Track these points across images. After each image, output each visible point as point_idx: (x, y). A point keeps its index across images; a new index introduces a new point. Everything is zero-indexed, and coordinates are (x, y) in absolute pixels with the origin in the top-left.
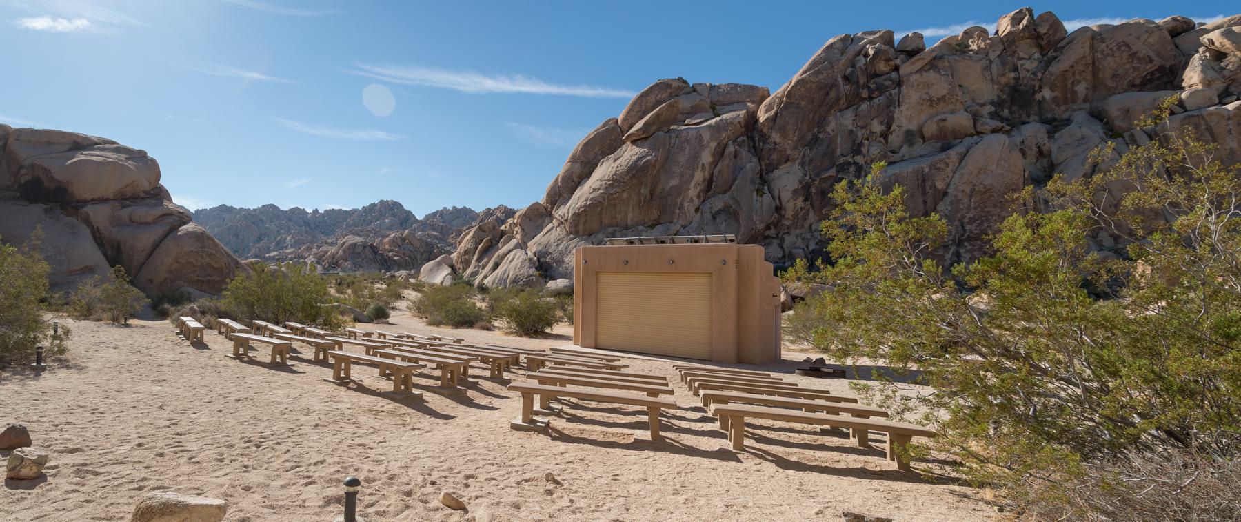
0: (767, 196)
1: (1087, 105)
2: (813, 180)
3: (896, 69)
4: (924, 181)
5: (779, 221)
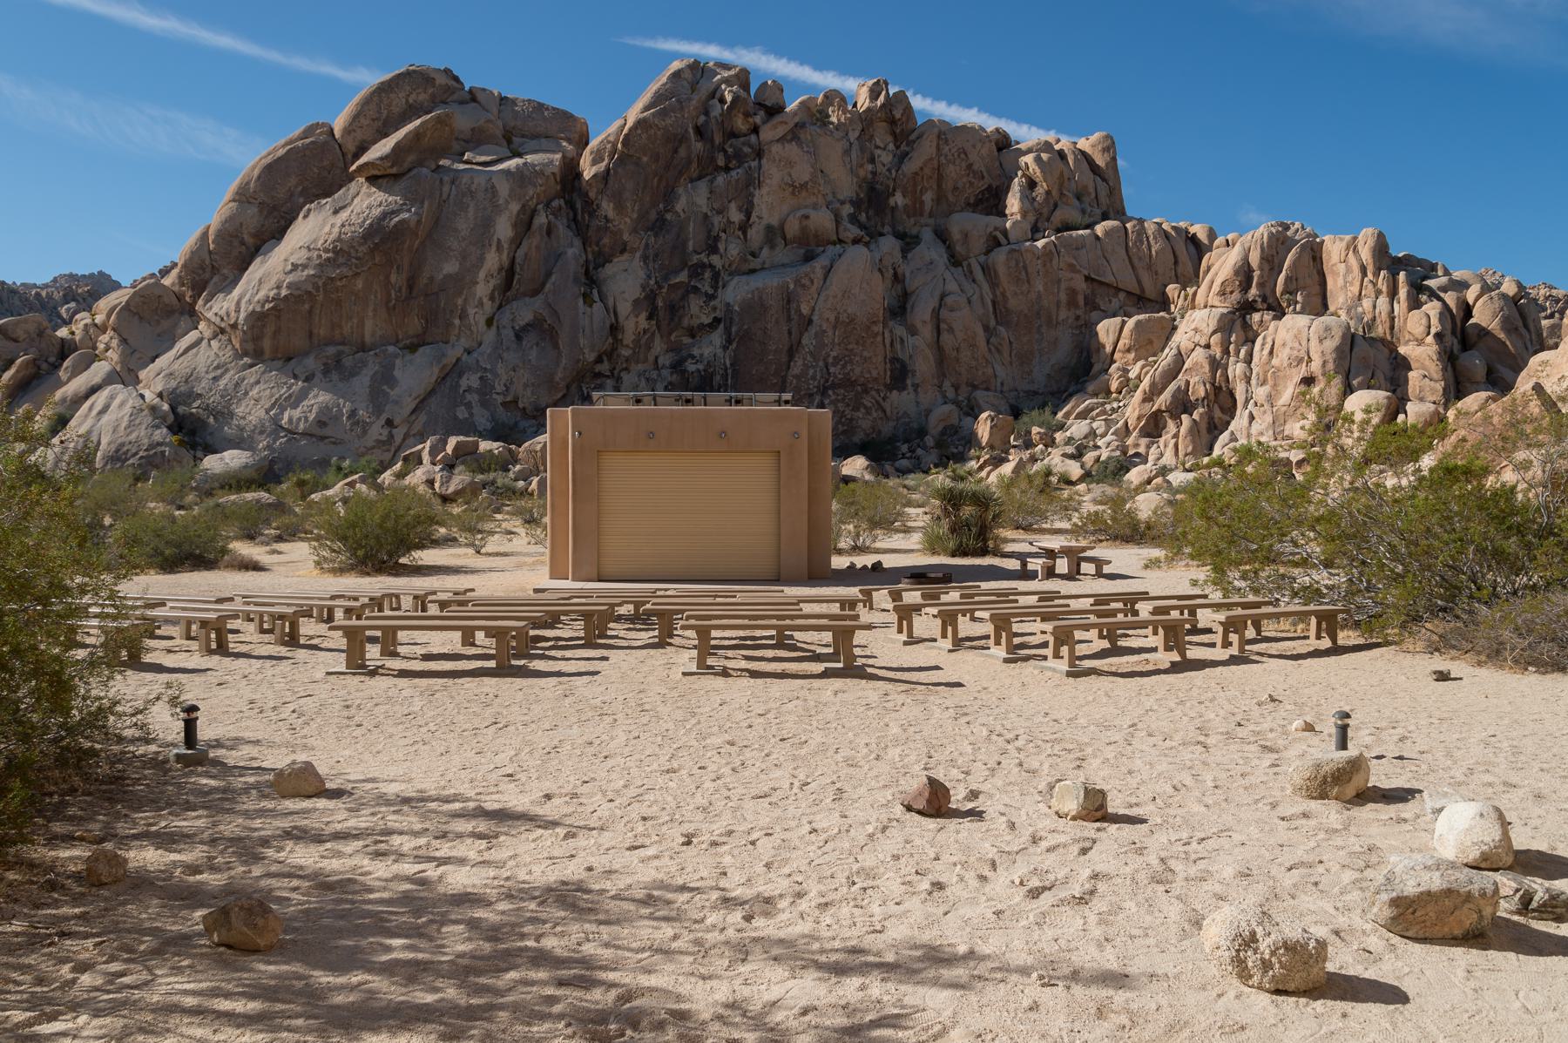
0: (598, 306)
1: (931, 221)
2: (660, 287)
3: (755, 130)
4: (789, 302)
5: (614, 349)
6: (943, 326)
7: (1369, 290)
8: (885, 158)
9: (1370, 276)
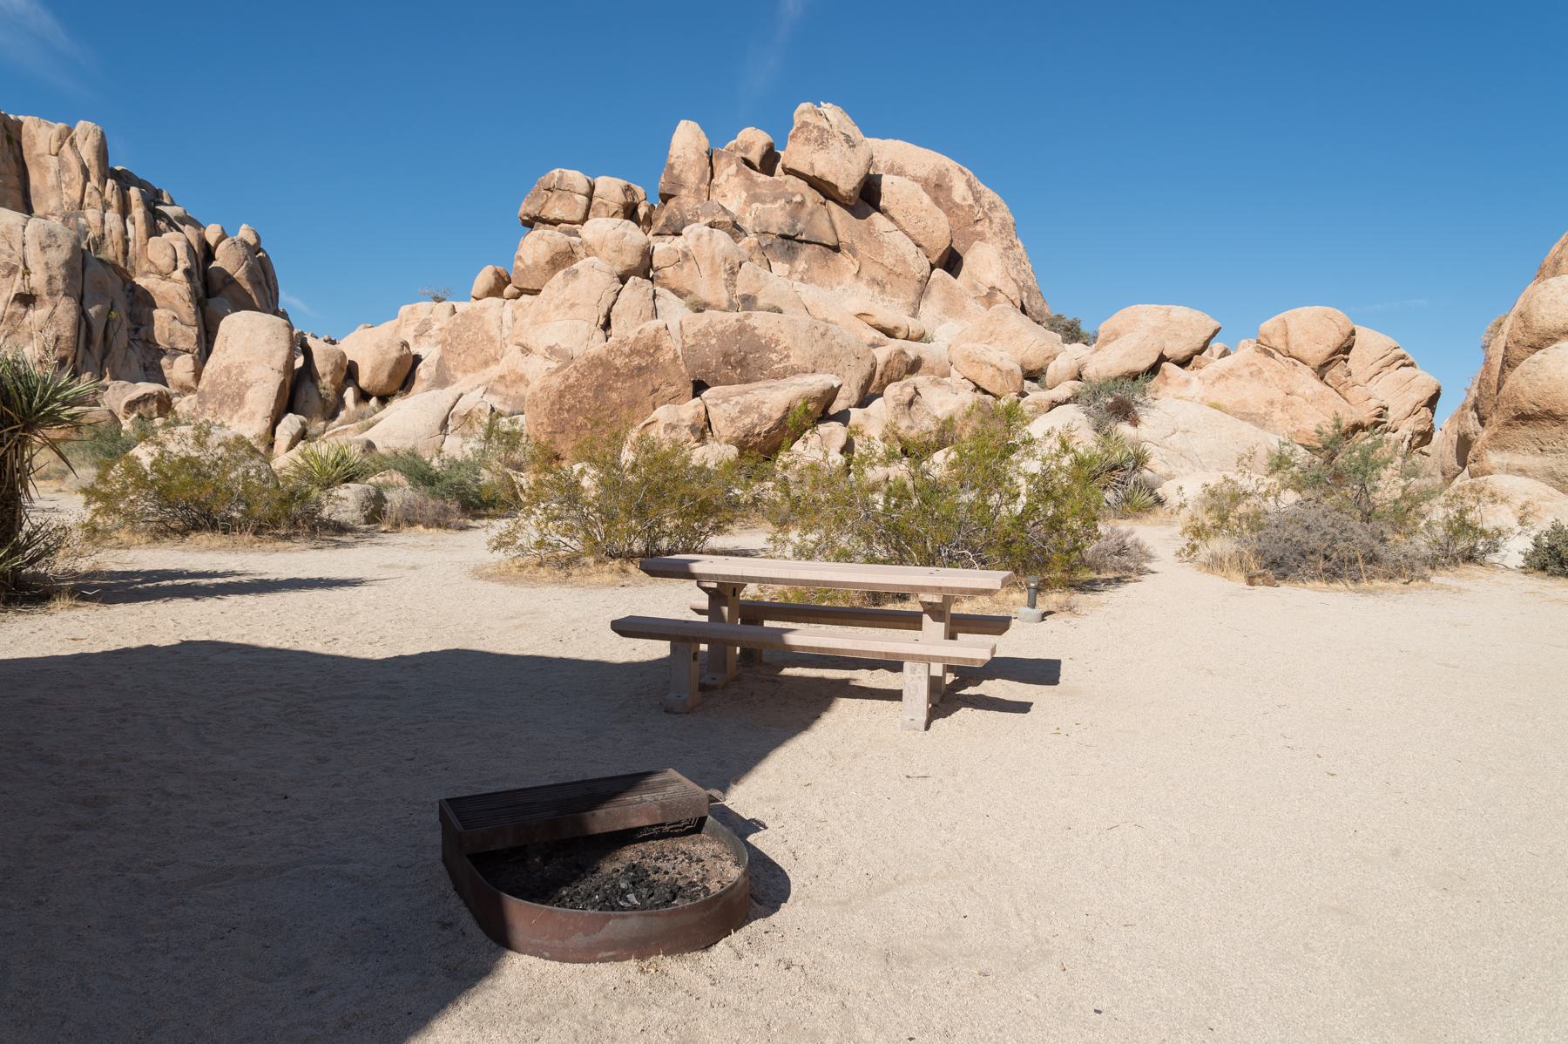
7: (92, 198)
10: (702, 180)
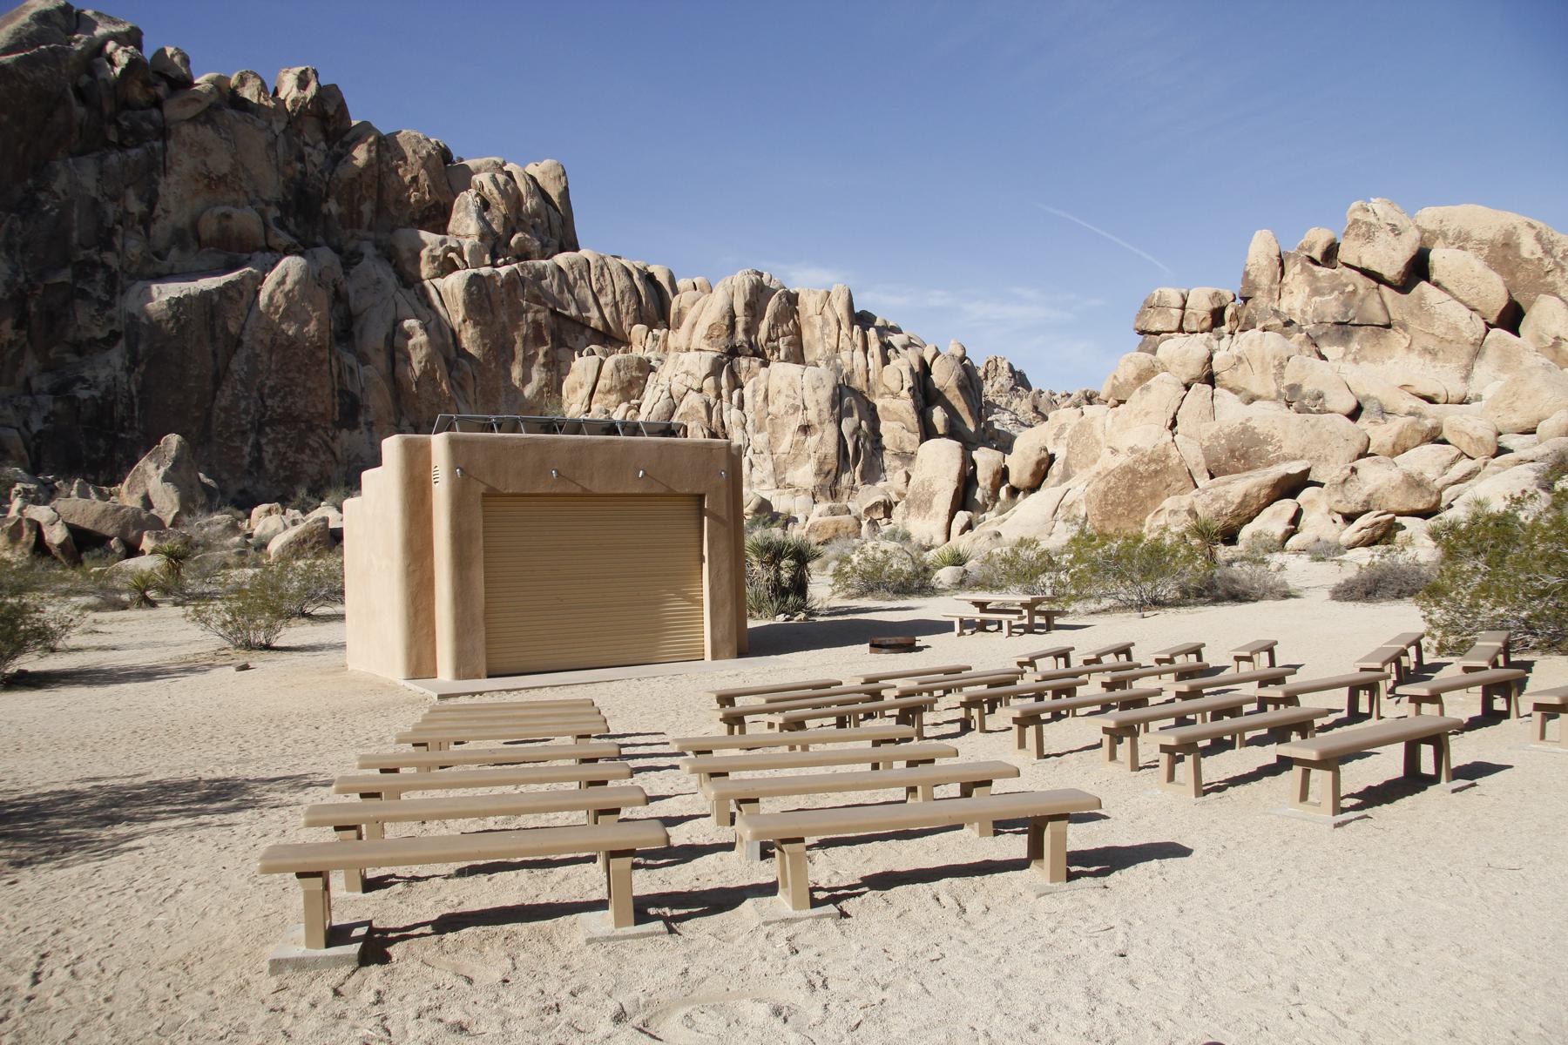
1: (371, 235)
2: (33, 287)
3: (158, 103)
4: (213, 317)
6: (398, 355)
7: (845, 343)
8: (317, 157)
9: (845, 330)
10: (1273, 281)
